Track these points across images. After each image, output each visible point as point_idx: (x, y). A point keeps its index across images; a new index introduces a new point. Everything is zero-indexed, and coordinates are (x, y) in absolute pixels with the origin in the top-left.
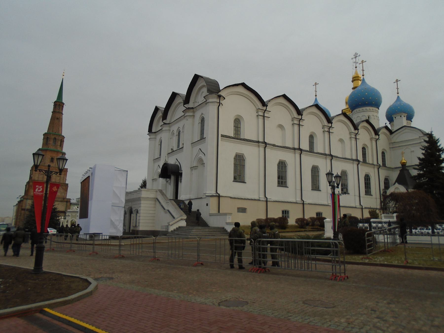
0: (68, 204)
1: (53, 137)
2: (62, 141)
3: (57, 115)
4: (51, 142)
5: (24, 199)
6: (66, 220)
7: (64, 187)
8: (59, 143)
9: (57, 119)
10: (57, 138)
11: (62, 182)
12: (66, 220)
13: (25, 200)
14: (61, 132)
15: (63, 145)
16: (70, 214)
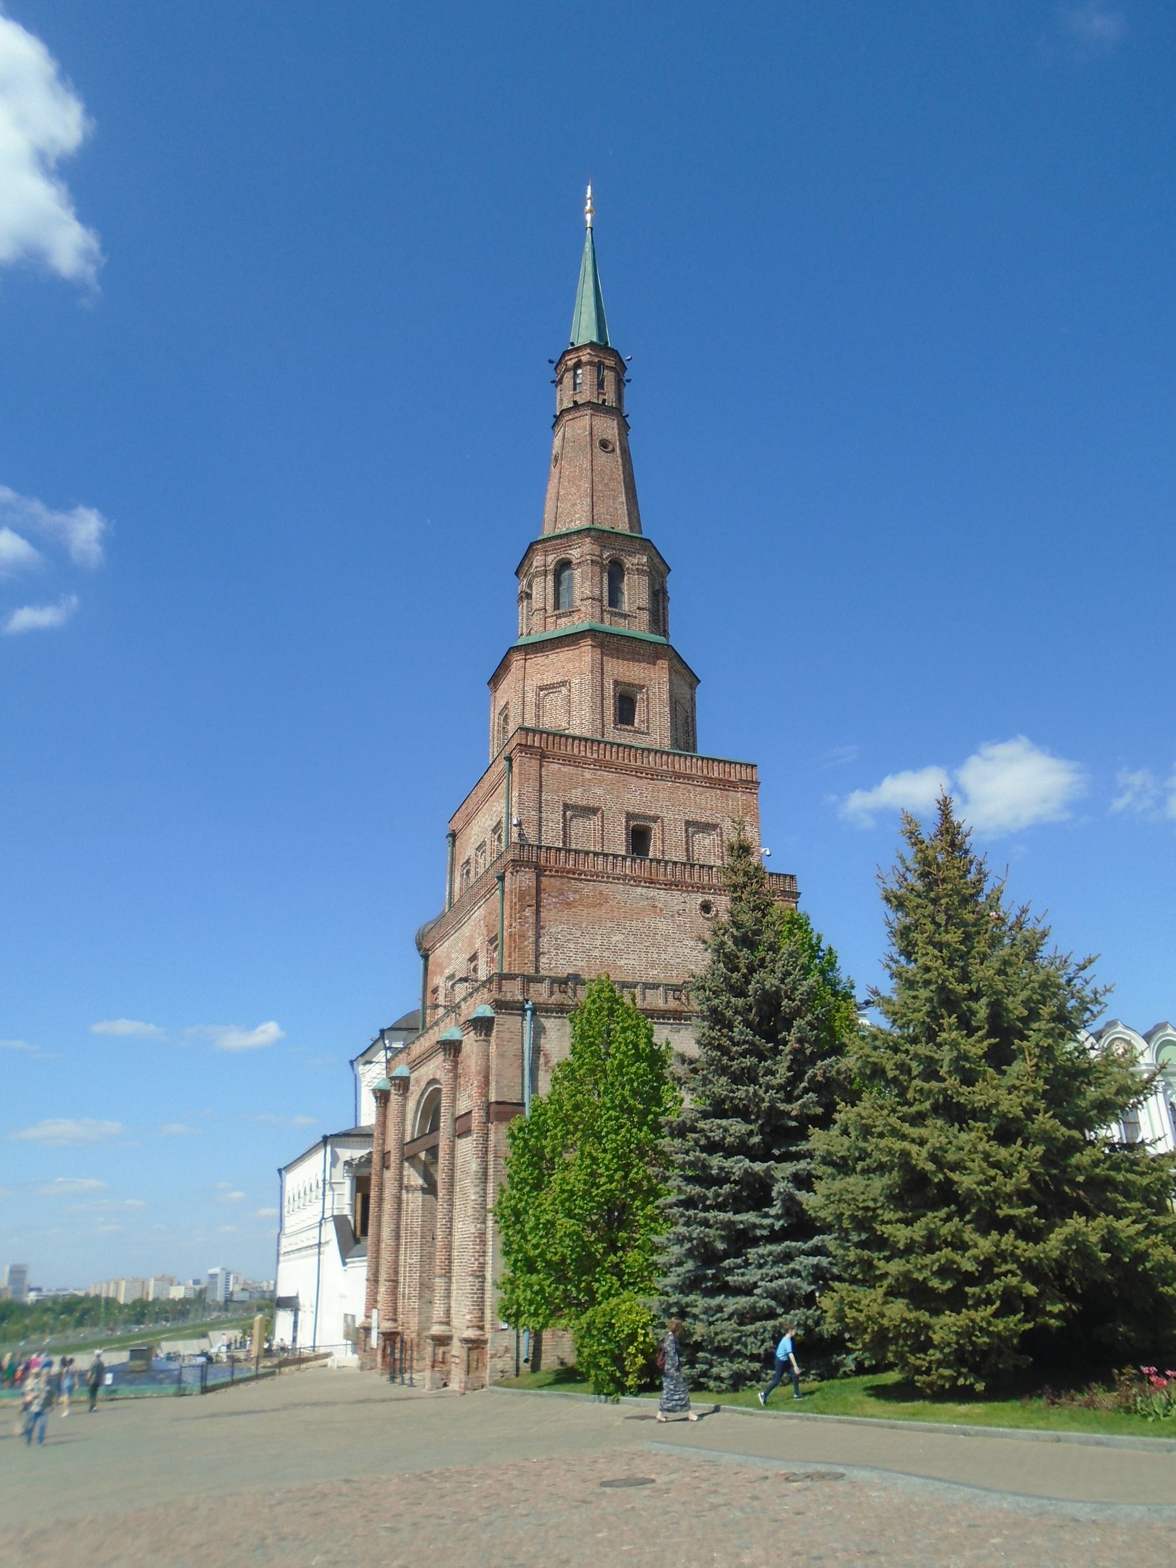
3: (608, 428)
5: (500, 1005)
9: (604, 444)
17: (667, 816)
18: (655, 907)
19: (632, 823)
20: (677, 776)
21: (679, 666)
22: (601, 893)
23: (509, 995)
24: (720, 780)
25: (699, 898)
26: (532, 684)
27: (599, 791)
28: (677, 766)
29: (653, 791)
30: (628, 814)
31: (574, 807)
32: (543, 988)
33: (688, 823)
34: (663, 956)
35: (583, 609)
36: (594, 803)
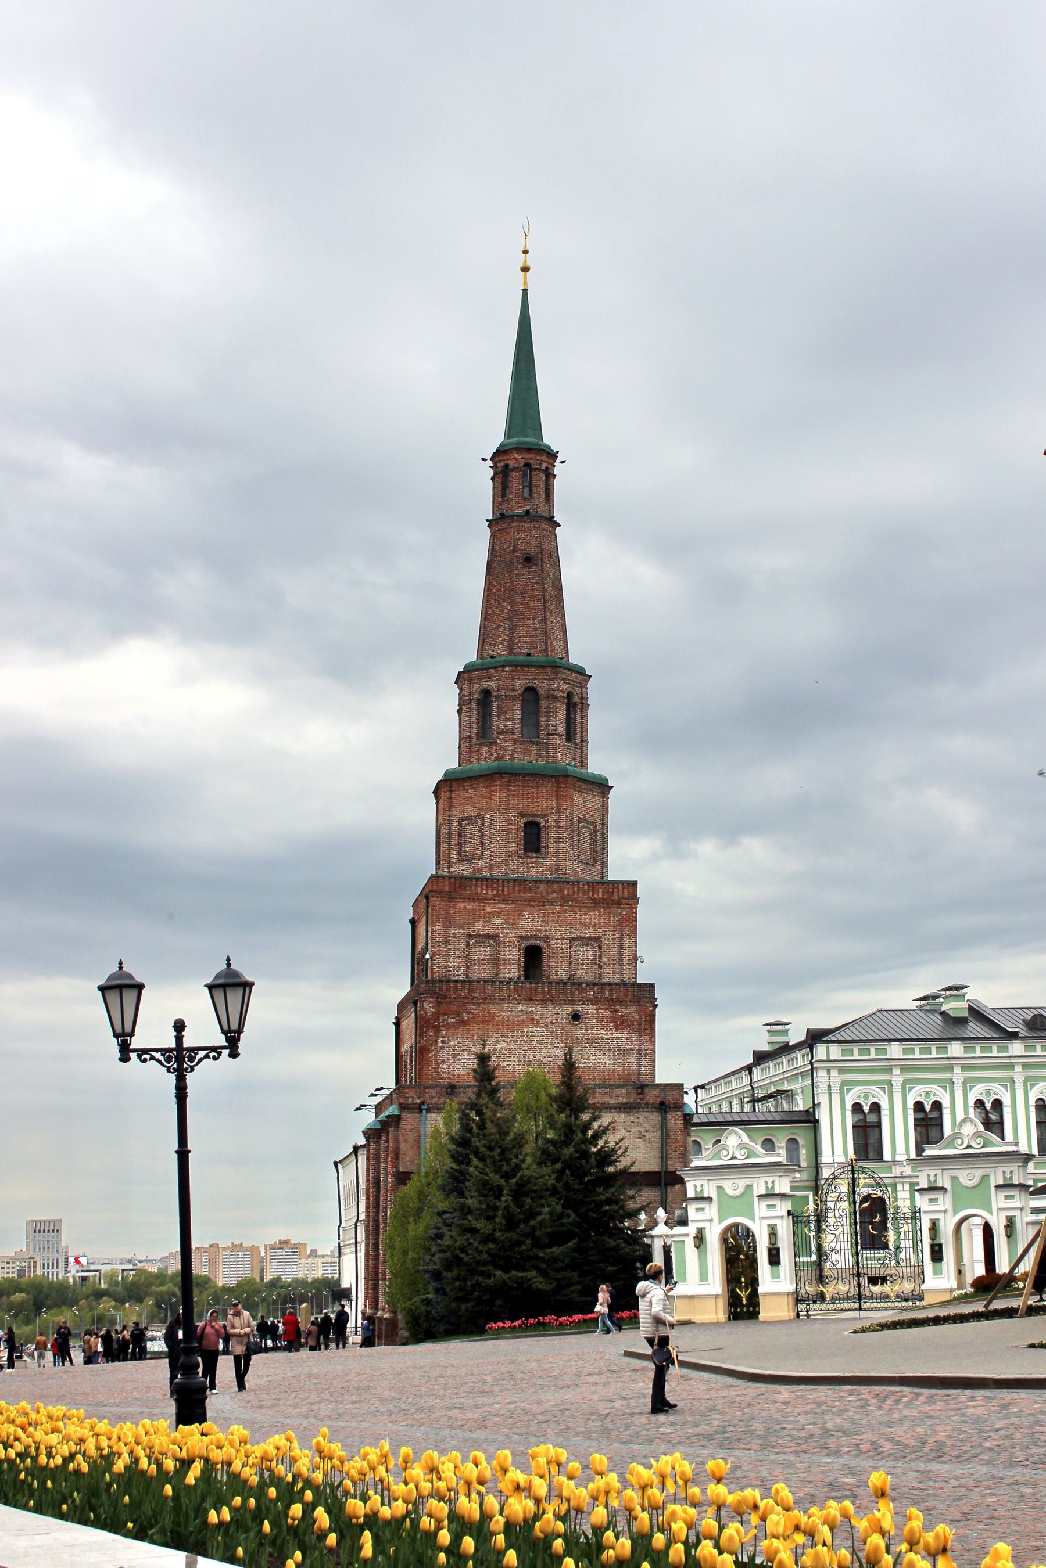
0: (675, 1121)
1: (520, 684)
2: (576, 706)
4: (509, 720)
5: (403, 1107)
6: (691, 1229)
7: (632, 1011)
8: (561, 716)
9: (528, 560)
10: (542, 686)
11: (610, 976)
12: (691, 1229)
13: (409, 1120)
14: (558, 645)
15: (584, 730)
16: (710, 1191)
17: (555, 935)
18: (533, 1019)
19: (525, 944)
20: (564, 900)
21: (584, 786)
22: (489, 1012)
23: (410, 1101)
24: (604, 900)
25: (568, 1009)
26: (457, 813)
27: (497, 921)
28: (566, 892)
29: (544, 916)
30: (521, 937)
31: (477, 936)
32: (433, 1093)
33: (573, 939)
34: (538, 1057)
35: (499, 742)
36: (491, 932)
